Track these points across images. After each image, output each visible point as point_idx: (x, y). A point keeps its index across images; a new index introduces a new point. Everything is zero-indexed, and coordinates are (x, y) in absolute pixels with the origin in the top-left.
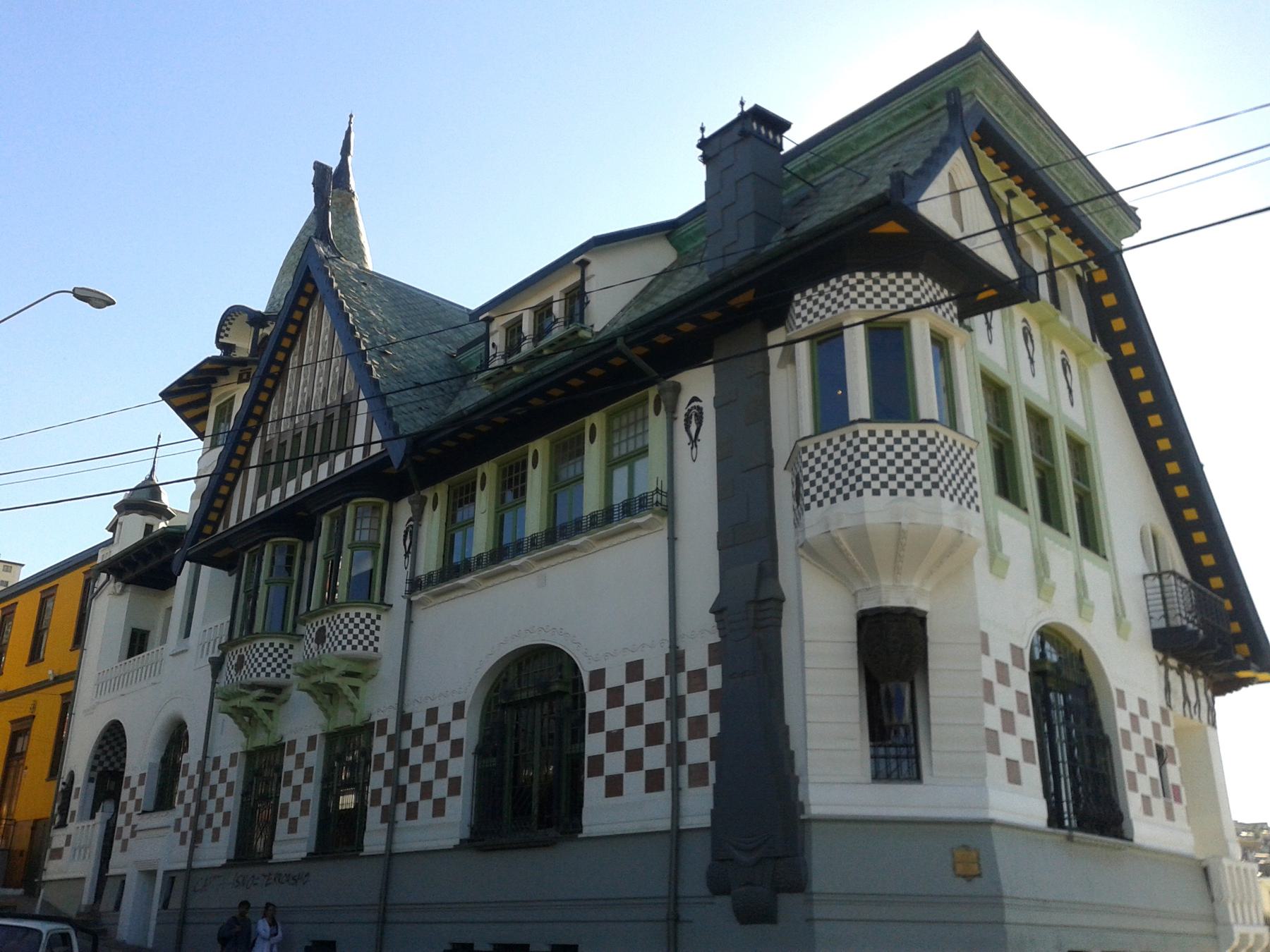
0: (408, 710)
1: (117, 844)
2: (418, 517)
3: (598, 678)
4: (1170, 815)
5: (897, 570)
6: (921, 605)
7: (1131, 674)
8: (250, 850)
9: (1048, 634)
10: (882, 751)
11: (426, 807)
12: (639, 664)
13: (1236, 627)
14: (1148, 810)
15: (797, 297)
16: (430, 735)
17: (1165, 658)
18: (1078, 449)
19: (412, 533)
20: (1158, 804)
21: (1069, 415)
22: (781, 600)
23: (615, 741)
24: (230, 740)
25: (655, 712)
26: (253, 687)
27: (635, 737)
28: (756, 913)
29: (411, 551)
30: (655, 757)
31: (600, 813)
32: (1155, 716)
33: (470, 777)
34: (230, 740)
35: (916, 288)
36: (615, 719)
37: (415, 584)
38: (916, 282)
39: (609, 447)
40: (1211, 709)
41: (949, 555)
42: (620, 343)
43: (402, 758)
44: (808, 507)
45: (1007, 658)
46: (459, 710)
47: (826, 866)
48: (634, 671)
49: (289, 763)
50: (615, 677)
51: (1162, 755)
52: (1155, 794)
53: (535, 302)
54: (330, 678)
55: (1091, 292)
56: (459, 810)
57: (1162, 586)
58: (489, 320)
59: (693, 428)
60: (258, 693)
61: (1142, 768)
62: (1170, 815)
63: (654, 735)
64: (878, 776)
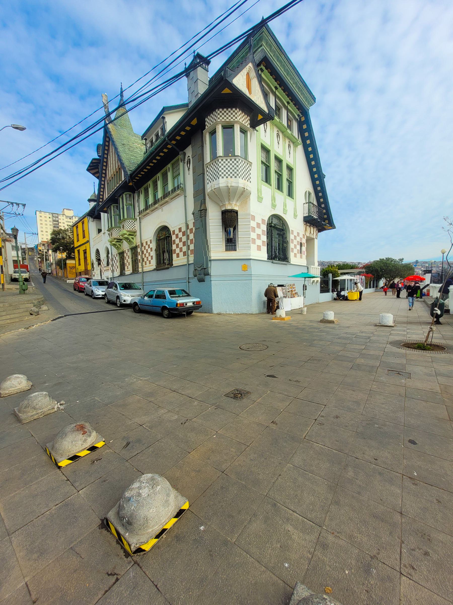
1: (102, 273)
2: (139, 196)
4: (301, 257)
5: (229, 200)
6: (236, 208)
8: (122, 274)
9: (275, 216)
10: (228, 244)
11: (148, 262)
13: (326, 216)
15: (206, 119)
18: (290, 169)
19: (138, 201)
20: (298, 255)
21: (287, 160)
22: (206, 210)
23: (177, 246)
24: (115, 251)
26: (115, 239)
27: (181, 245)
28: (201, 280)
29: (139, 206)
30: (185, 249)
31: (176, 261)
32: (301, 236)
34: (115, 251)
35: (236, 114)
36: (177, 241)
37: (140, 213)
38: (236, 111)
39: (173, 173)
41: (243, 195)
42: (167, 139)
43: (143, 252)
45: (260, 222)
47: (214, 269)
48: (180, 230)
49: (125, 255)
50: (177, 232)
51: (301, 245)
52: (298, 253)
53: (155, 133)
54: (126, 236)
55: (300, 124)
60: (115, 240)
62: (301, 257)
63: (184, 244)
64: (227, 250)
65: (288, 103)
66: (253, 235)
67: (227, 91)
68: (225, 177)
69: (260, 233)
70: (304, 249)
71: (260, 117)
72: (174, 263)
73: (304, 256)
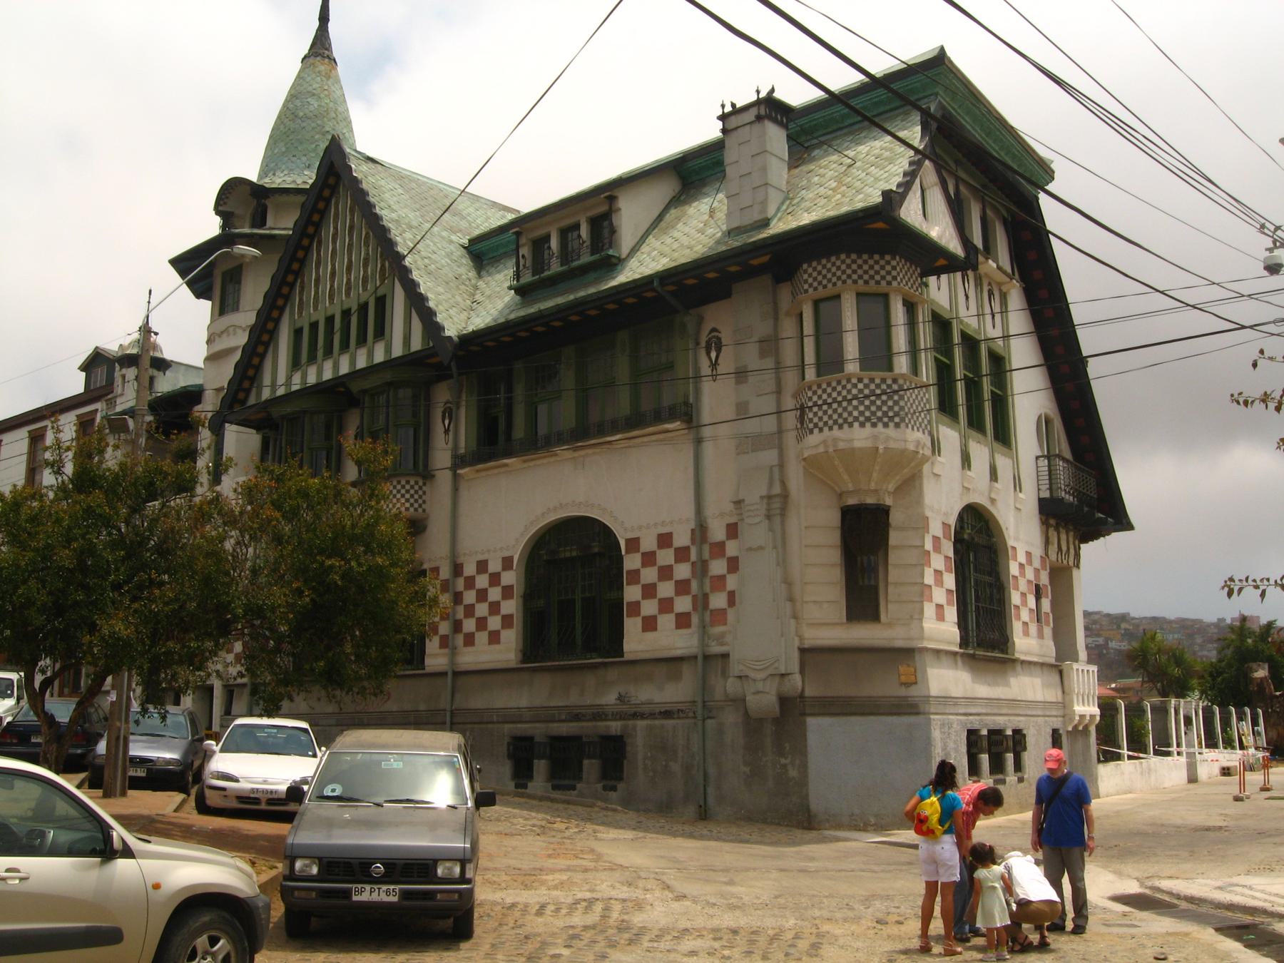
0: (459, 562)
3: (633, 544)
4: (1041, 635)
7: (1022, 535)
12: (670, 535)
14: (1026, 633)
15: (805, 266)
16: (482, 582)
17: (1047, 520)
20: (1033, 628)
25: (683, 571)
31: (635, 641)
32: (1037, 563)
33: (521, 615)
37: (459, 461)
38: (894, 263)
40: (1077, 555)
44: (811, 432)
45: (939, 533)
46: (507, 563)
48: (665, 540)
50: (648, 543)
56: (511, 641)
57: (1049, 466)
58: (518, 234)
59: (713, 355)
61: (1024, 603)
65: (984, 186)
66: (929, 579)
67: (880, 225)
68: (868, 425)
69: (941, 567)
70: (1046, 604)
71: (942, 262)
72: (626, 647)
73: (1048, 631)
